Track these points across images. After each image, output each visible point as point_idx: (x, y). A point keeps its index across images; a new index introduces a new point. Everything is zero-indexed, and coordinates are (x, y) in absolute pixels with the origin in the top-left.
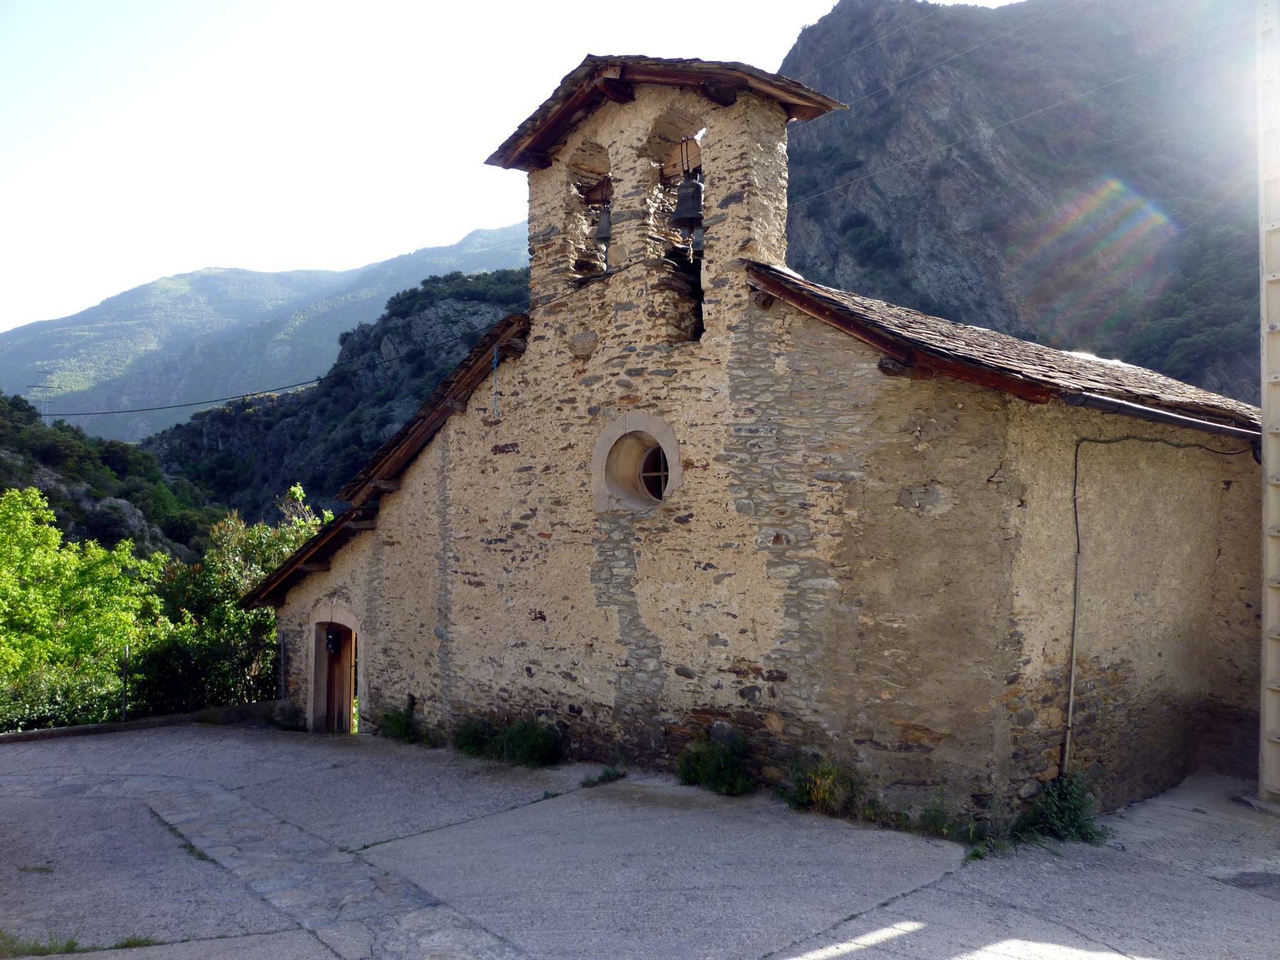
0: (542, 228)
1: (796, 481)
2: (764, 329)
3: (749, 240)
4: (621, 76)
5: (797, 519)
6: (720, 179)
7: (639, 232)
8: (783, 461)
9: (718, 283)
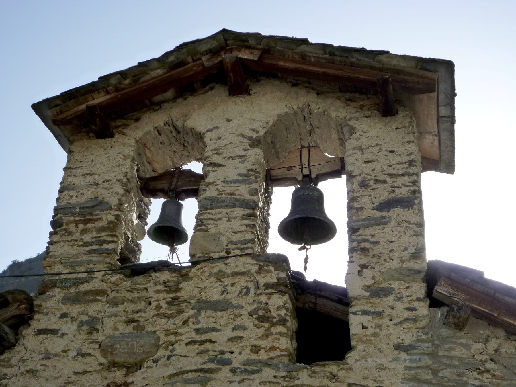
0: (82, 200)
2: (458, 352)
4: (260, 58)
6: (377, 181)
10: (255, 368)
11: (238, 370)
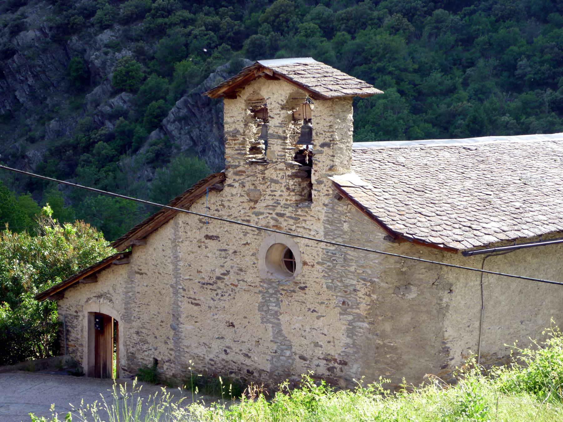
1: (352, 279)
2: (339, 209)
3: (333, 166)
5: (352, 295)
7: (282, 147)
8: (346, 269)
9: (319, 182)
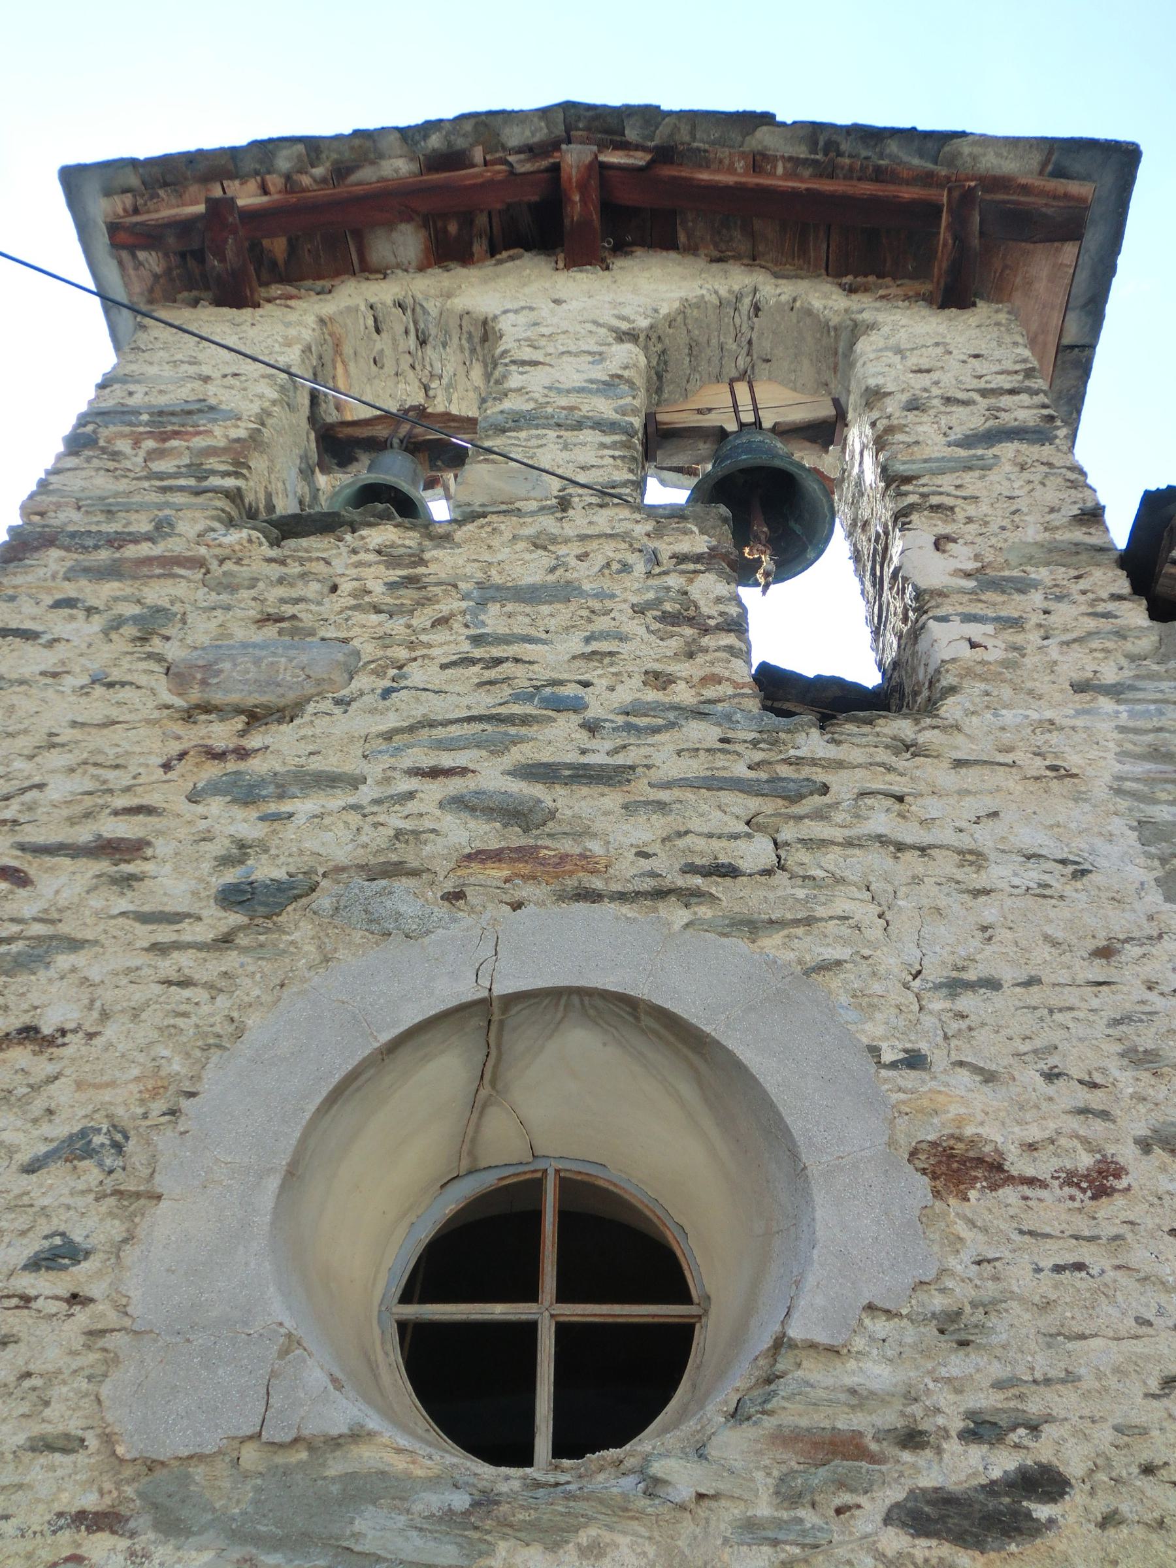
10: (660, 722)
11: (607, 724)
